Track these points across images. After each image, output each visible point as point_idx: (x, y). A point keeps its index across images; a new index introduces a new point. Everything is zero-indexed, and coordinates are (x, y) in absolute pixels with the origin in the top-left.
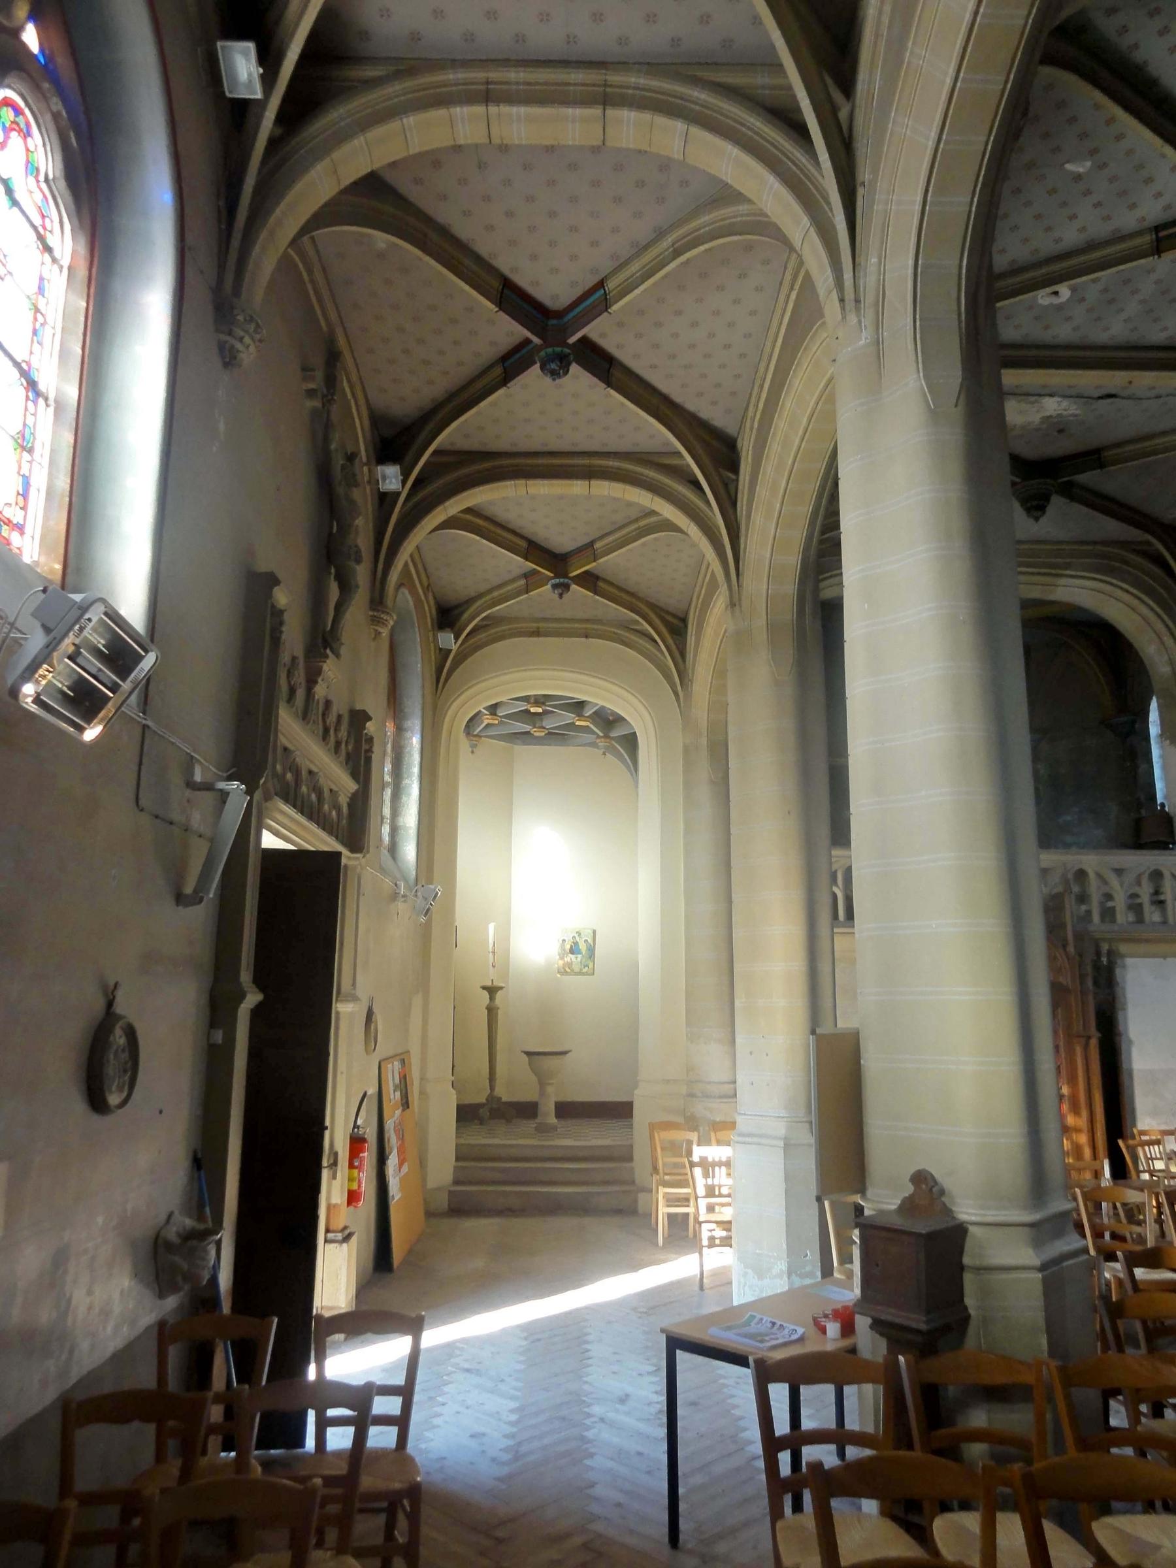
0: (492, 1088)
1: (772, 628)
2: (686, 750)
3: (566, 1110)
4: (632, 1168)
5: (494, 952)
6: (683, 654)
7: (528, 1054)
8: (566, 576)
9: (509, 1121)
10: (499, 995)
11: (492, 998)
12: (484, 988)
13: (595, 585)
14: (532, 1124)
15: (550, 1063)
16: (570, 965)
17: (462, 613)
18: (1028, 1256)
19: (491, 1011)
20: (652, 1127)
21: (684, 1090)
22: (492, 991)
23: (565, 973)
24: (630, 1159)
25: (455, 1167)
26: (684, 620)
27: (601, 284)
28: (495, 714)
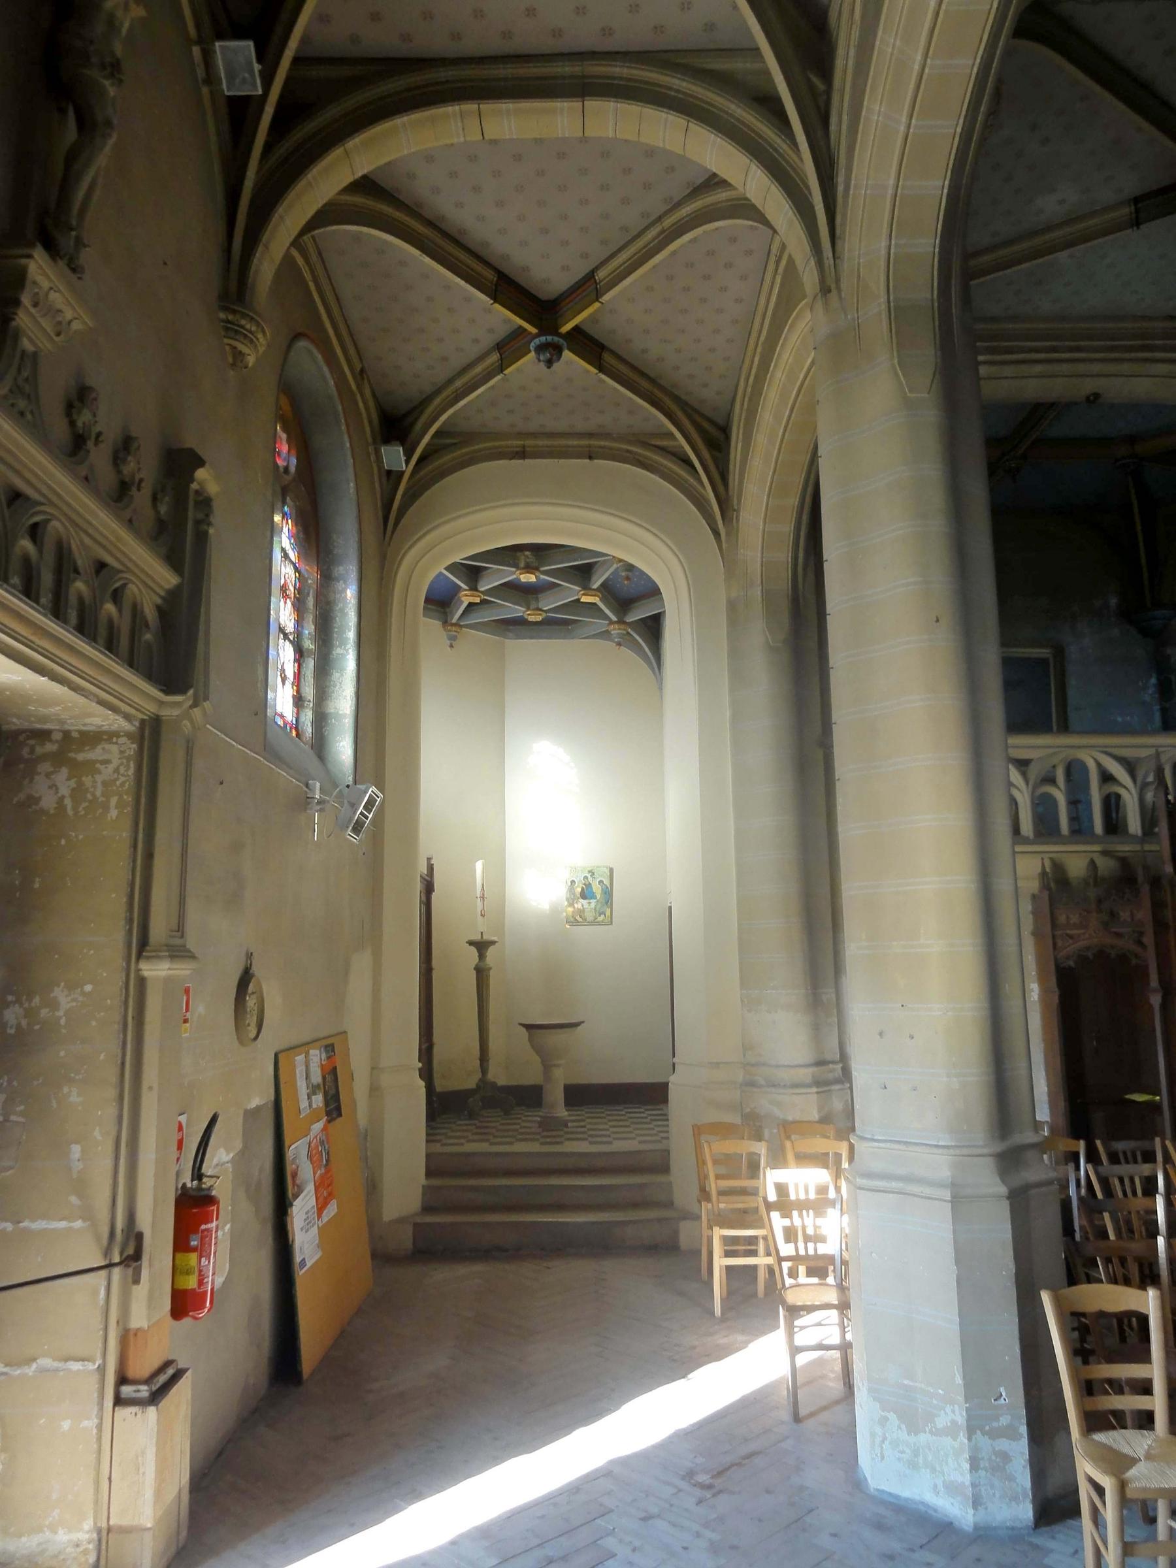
0: (484, 1070)
1: (898, 313)
2: (732, 606)
3: (578, 1096)
4: (670, 1184)
5: (483, 897)
7: (529, 1027)
10: (491, 952)
11: (482, 956)
12: (471, 943)
13: (600, 358)
14: (535, 1116)
16: (581, 912)
17: (412, 424)
19: (481, 973)
20: (698, 1130)
21: (740, 1077)
22: (481, 946)
23: (575, 923)
25: (426, 1190)
26: (725, 430)
28: (476, 589)
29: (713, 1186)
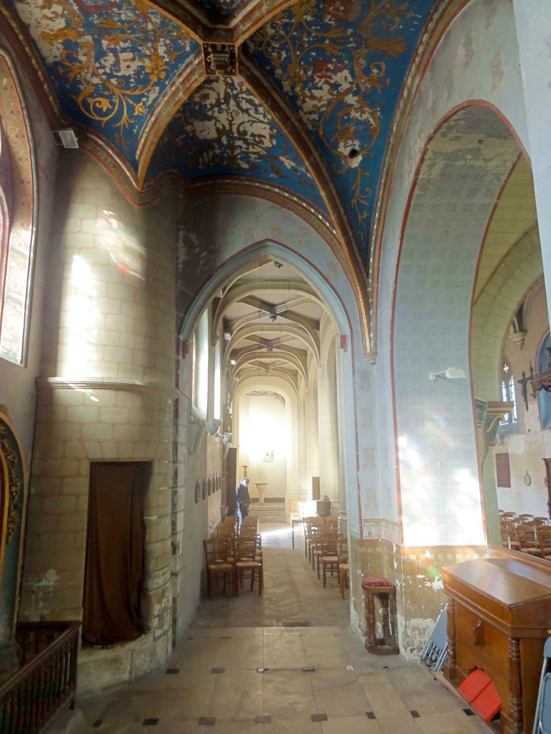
2: (298, 405)
3: (266, 500)
6: (297, 381)
7: (256, 484)
8: (268, 369)
14: (257, 504)
15: (262, 486)
22: (245, 467)
24: (285, 510)
27: (279, 338)
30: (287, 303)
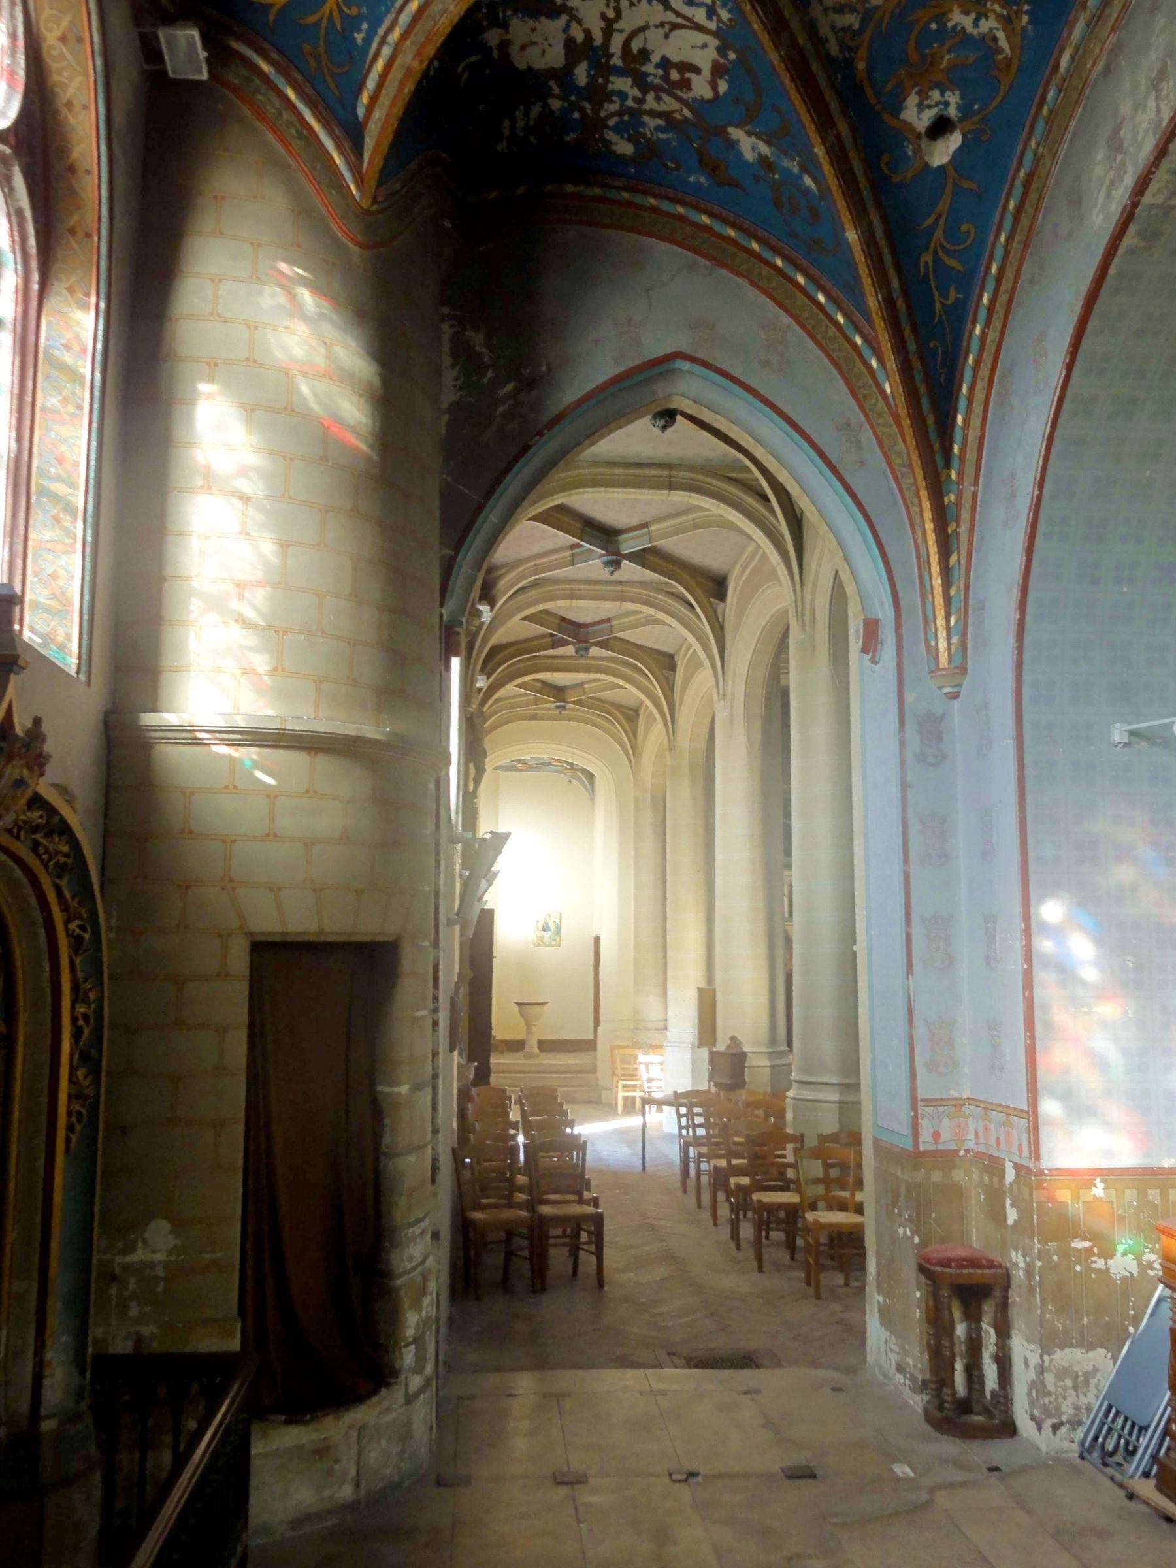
1: (692, 766)
2: (636, 800)
3: (544, 1046)
6: (635, 734)
7: (518, 1004)
8: (564, 700)
9: (502, 1052)
14: (520, 1054)
18: (766, 1062)
20: (612, 1048)
23: (539, 945)
24: (595, 1072)
27: (608, 620)
29: (619, 1071)
30: (653, 527)
